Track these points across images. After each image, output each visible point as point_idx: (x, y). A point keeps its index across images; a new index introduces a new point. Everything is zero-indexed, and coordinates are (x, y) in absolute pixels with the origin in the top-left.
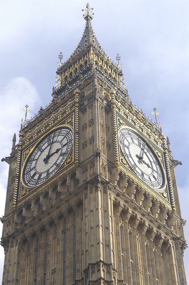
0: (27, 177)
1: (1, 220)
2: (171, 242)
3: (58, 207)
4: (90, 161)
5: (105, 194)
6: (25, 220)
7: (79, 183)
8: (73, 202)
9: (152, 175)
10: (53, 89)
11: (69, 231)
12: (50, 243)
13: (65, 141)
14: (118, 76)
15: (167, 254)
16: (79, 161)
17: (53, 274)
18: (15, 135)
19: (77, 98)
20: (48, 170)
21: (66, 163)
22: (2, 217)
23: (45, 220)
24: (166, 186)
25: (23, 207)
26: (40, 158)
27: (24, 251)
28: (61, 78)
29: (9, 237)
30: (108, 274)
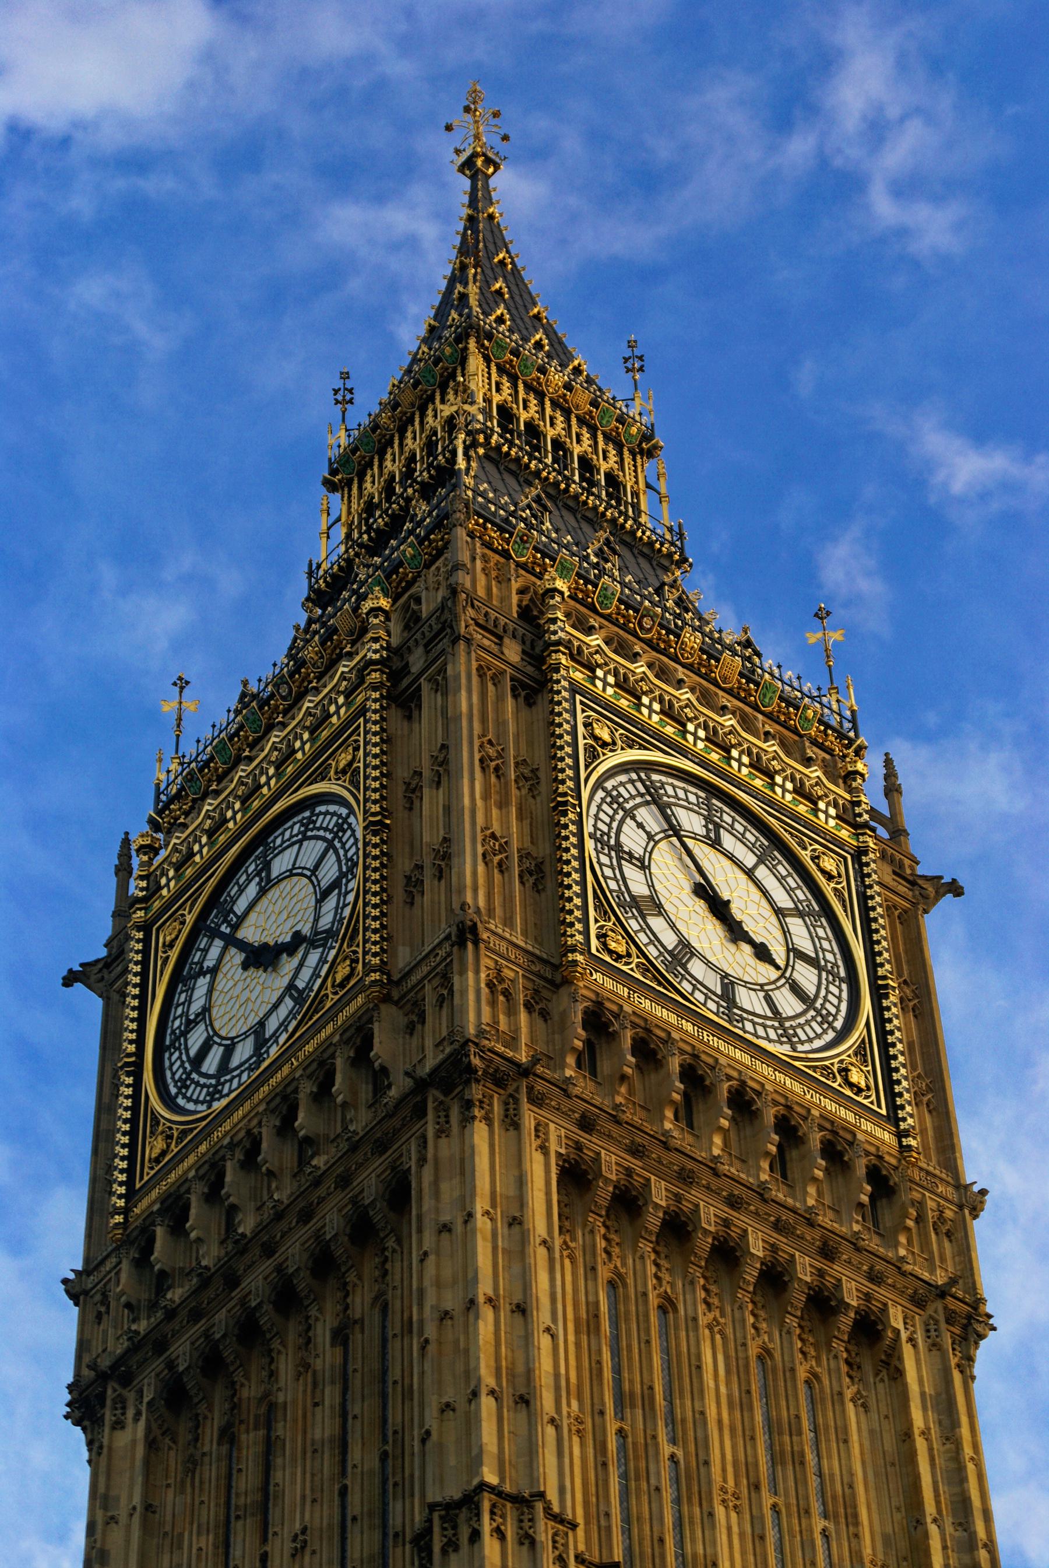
0: (176, 1064)
1: (67, 1292)
2: (896, 1318)
3: (306, 1216)
4: (435, 968)
5: (512, 1133)
6: (169, 1289)
7: (389, 1086)
8: (370, 1182)
9: (783, 981)
10: (310, 574)
11: (363, 1332)
12: (281, 1398)
13: (329, 872)
14: (634, 460)
15: (882, 1380)
16: (383, 973)
17: (298, 1557)
18: (126, 842)
19: (376, 640)
20: (262, 1024)
21: (333, 986)
22: (72, 1276)
23: (256, 1282)
24: (867, 1024)
25: (153, 1224)
26: (224, 961)
27: (174, 1441)
28: (344, 508)
29: (103, 1377)
30: (525, 1548)
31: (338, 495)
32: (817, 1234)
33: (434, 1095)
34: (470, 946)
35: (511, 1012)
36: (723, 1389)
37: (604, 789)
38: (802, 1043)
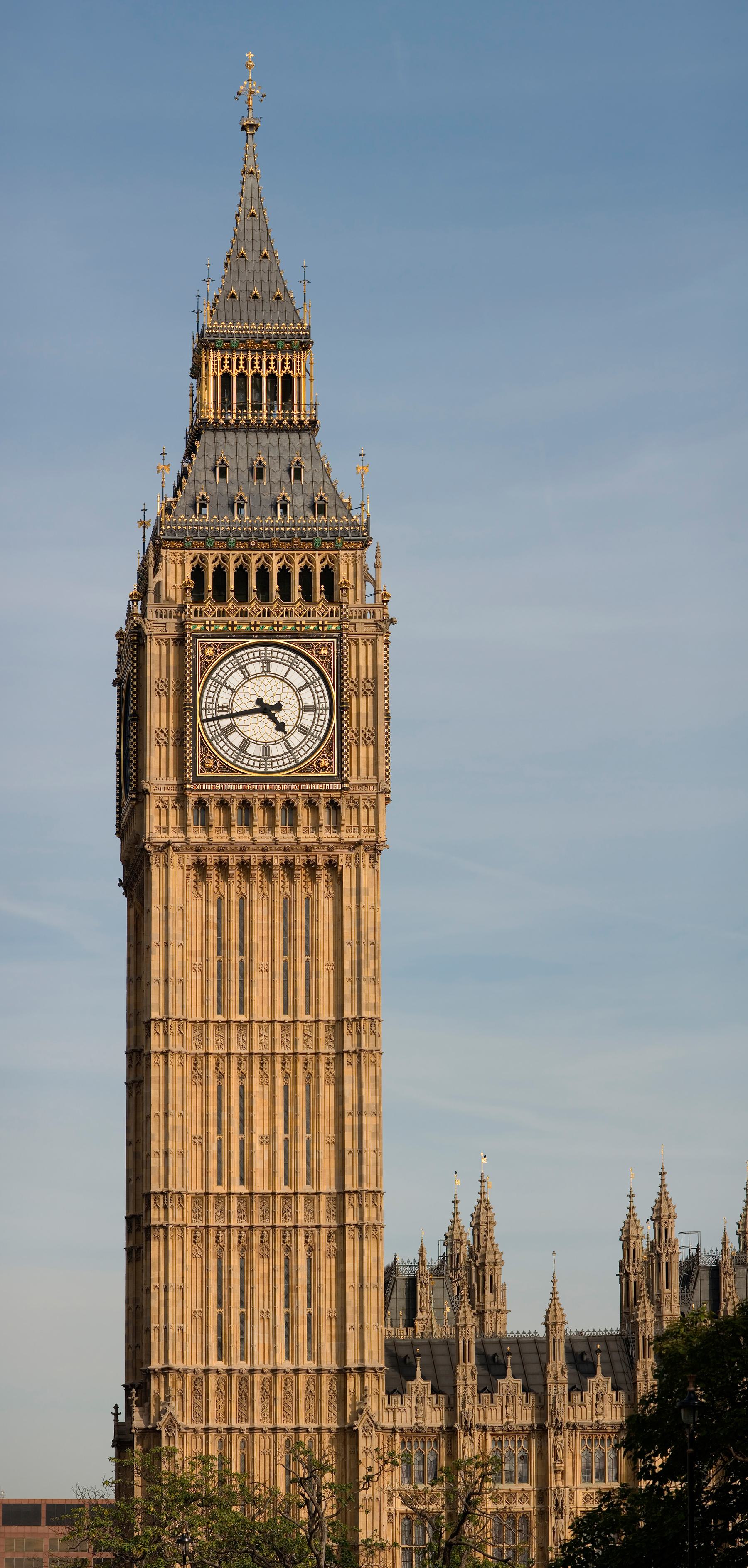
36: (265, 922)
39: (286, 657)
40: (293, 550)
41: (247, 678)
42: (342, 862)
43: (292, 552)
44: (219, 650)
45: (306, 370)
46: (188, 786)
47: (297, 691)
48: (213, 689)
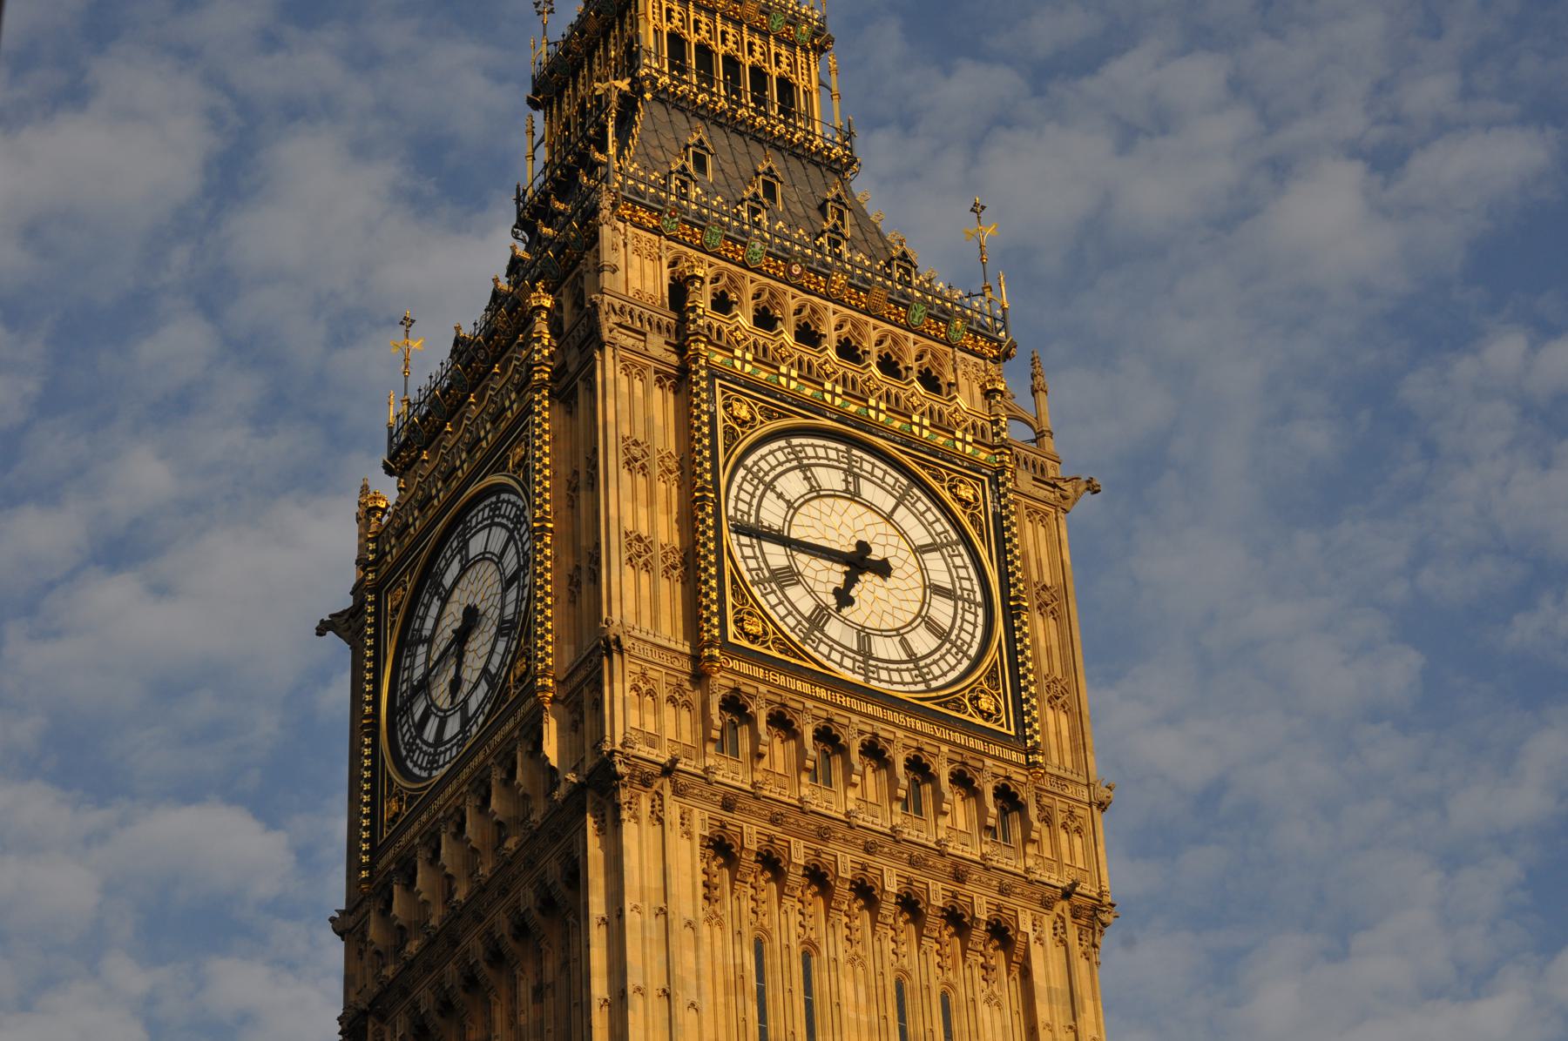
10: (518, 200)
22: (337, 915)
31: (542, 112)
32: (948, 861)
33: (590, 795)
34: (615, 656)
35: (657, 711)
36: (863, 1018)
37: (745, 468)
38: (936, 678)
39: (889, 479)
40: (867, 312)
41: (816, 492)
42: (1025, 924)
43: (864, 317)
44: (759, 417)
45: (821, 84)
46: (716, 652)
47: (920, 550)
48: (746, 486)
